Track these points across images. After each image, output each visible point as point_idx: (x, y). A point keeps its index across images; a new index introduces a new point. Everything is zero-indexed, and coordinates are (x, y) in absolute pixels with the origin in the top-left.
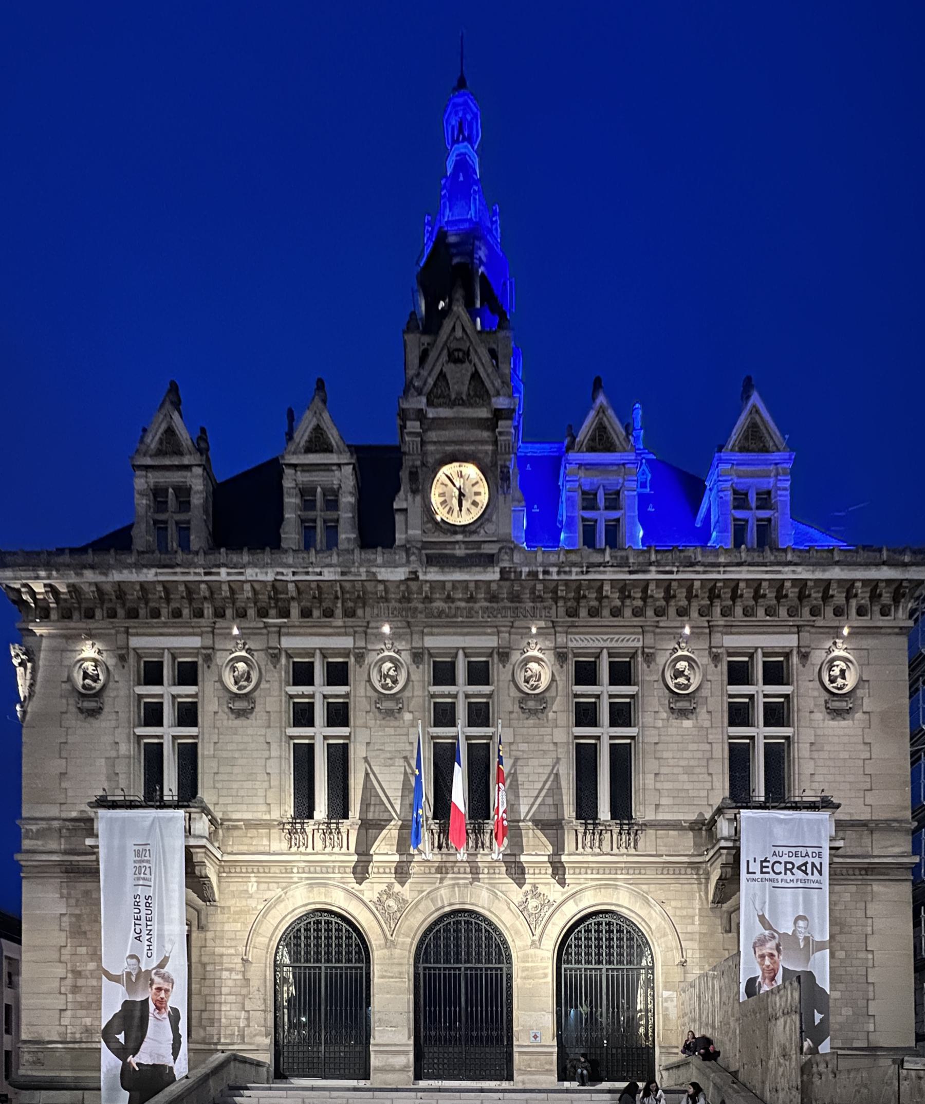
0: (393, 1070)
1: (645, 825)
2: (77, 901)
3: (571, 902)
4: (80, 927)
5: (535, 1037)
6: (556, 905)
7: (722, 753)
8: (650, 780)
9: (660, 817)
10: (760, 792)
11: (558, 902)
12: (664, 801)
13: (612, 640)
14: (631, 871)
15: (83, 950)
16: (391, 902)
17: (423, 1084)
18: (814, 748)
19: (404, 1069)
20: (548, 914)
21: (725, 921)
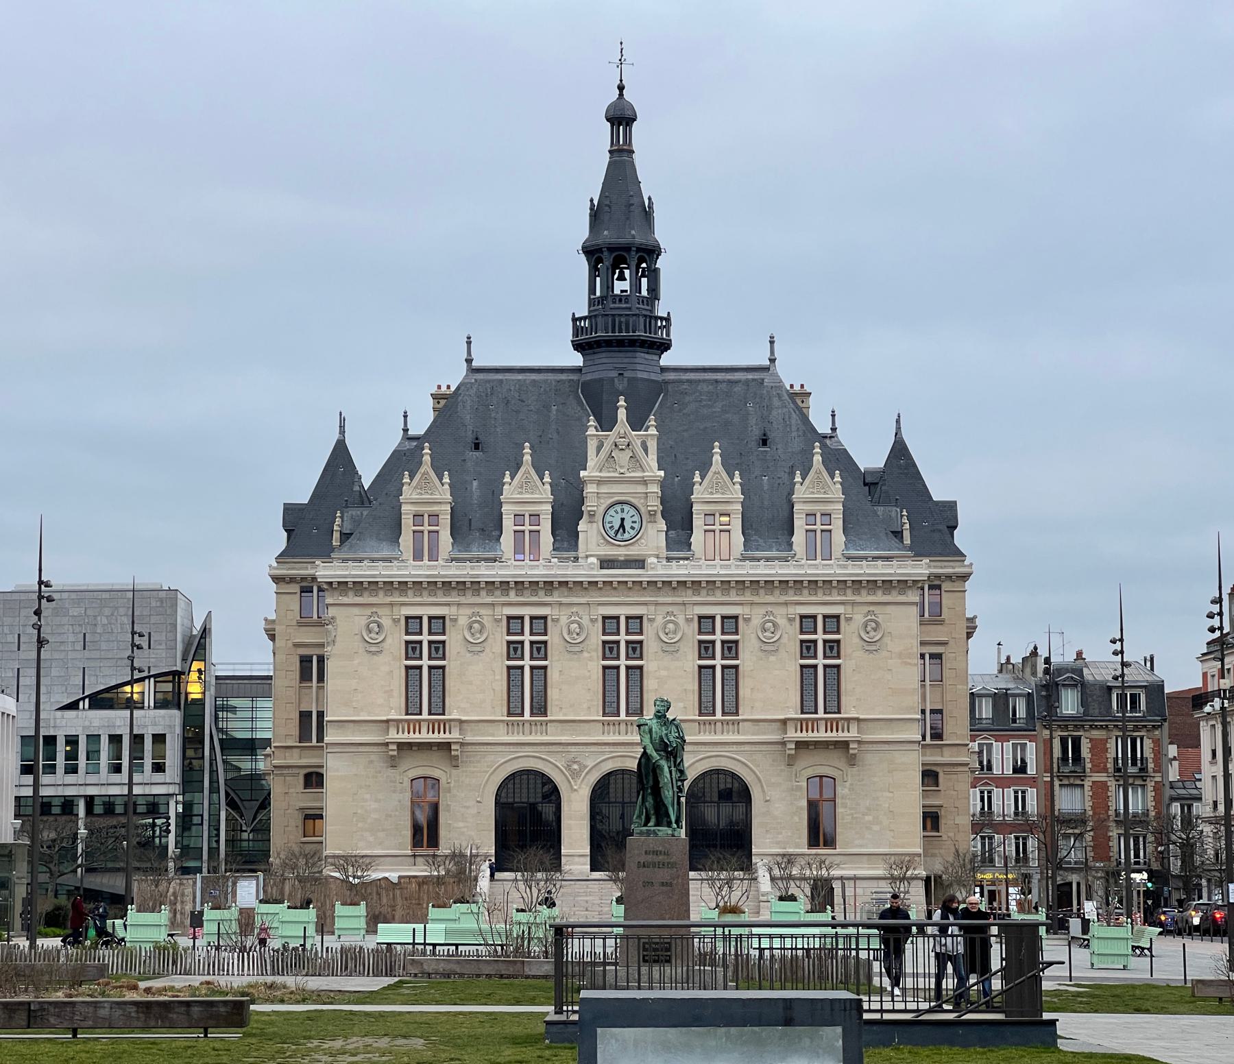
15: (368, 796)
16: (576, 767)
17: (597, 875)
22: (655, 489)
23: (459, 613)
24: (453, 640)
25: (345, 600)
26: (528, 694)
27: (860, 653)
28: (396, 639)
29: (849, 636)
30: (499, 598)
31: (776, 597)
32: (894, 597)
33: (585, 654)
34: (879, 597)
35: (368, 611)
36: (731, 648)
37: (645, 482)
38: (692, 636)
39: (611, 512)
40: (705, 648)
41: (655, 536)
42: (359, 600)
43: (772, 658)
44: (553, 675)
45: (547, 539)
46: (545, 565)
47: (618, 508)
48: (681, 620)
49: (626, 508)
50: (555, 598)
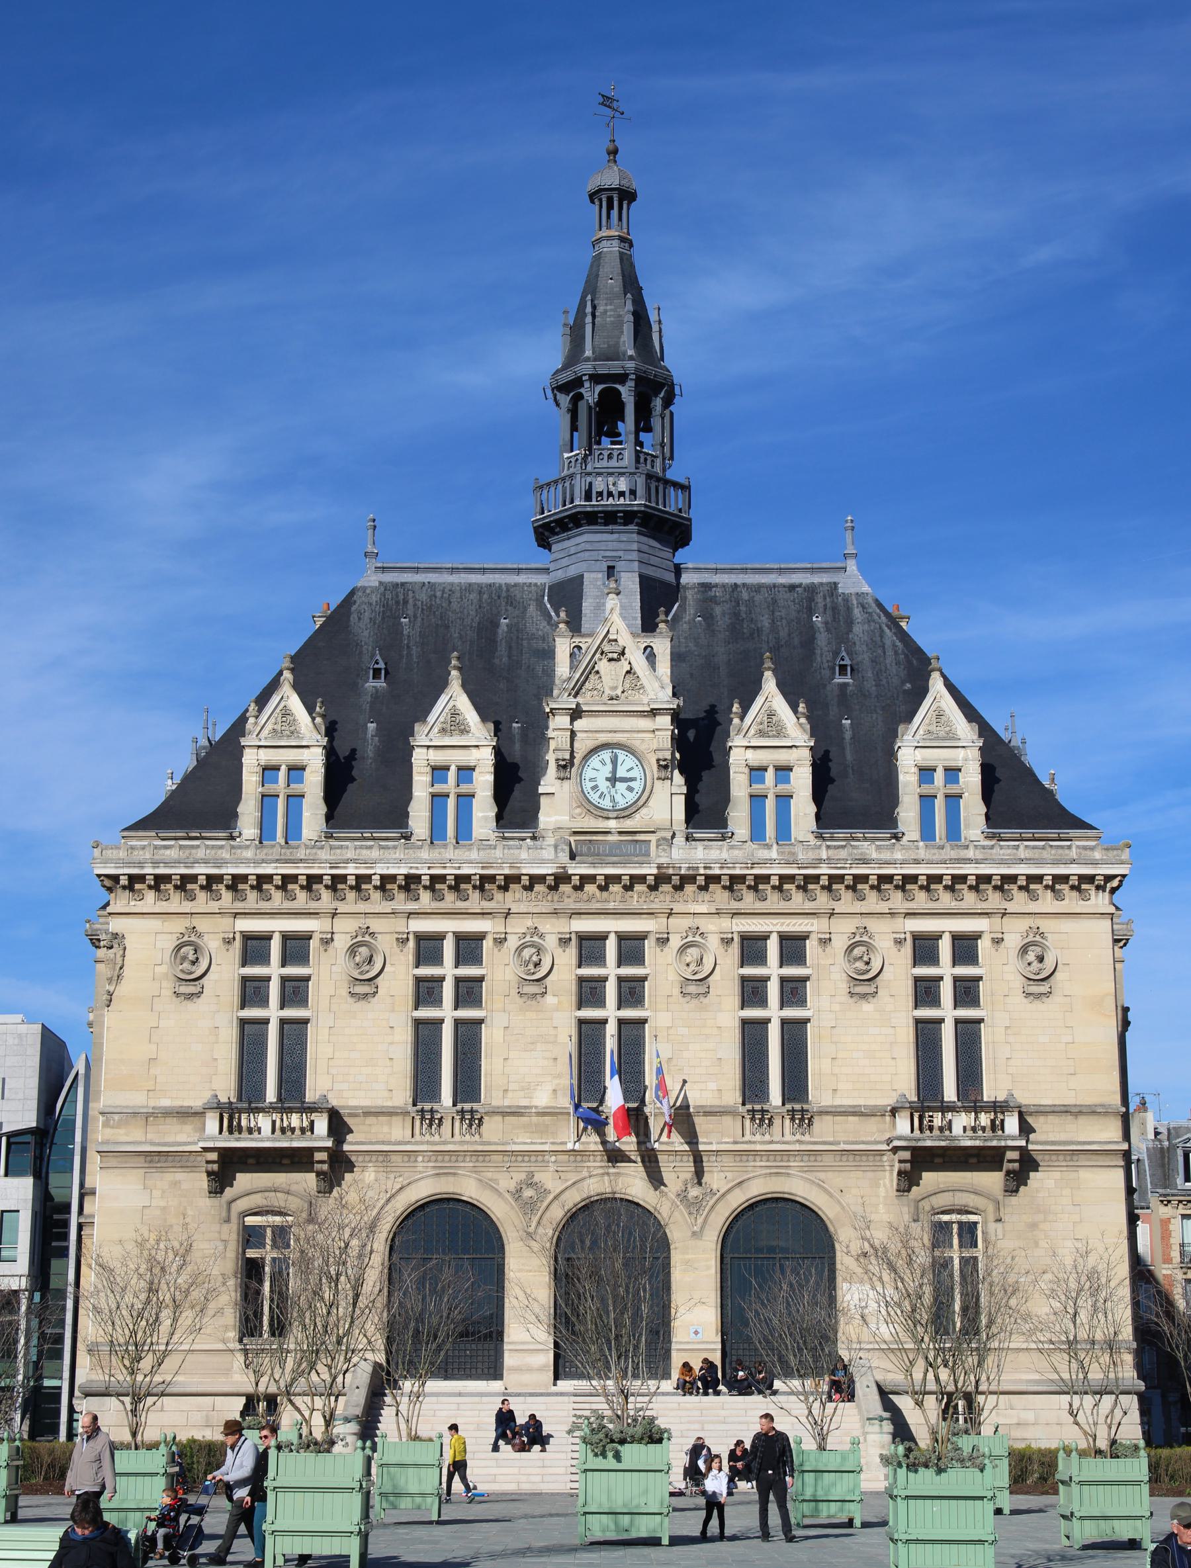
0: (530, 1370)
1: (823, 1112)
2: (163, 1192)
3: (737, 1191)
4: (165, 1220)
5: (696, 1333)
6: (718, 1195)
7: (907, 1035)
8: (826, 1065)
9: (837, 1102)
10: (950, 1092)
11: (722, 1191)
12: (841, 1086)
13: (782, 924)
14: (806, 1158)
17: (565, 1385)
18: (1009, 1031)
19: (541, 1369)
20: (711, 1203)
21: (912, 1209)
22: (665, 721)
23: (333, 925)
24: (327, 972)
25: (139, 906)
26: (447, 1068)
27: (1018, 999)
28: (226, 971)
29: (998, 969)
30: (401, 902)
31: (872, 902)
32: (1071, 901)
33: (550, 999)
34: (1047, 902)
35: (180, 925)
36: (793, 991)
37: (654, 713)
38: (728, 972)
39: (595, 761)
40: (752, 991)
41: (667, 802)
42: (163, 906)
43: (867, 1007)
44: (488, 1036)
45: (484, 810)
46: (485, 846)
47: (606, 755)
48: (713, 942)
49: (622, 755)
50: (501, 901)
